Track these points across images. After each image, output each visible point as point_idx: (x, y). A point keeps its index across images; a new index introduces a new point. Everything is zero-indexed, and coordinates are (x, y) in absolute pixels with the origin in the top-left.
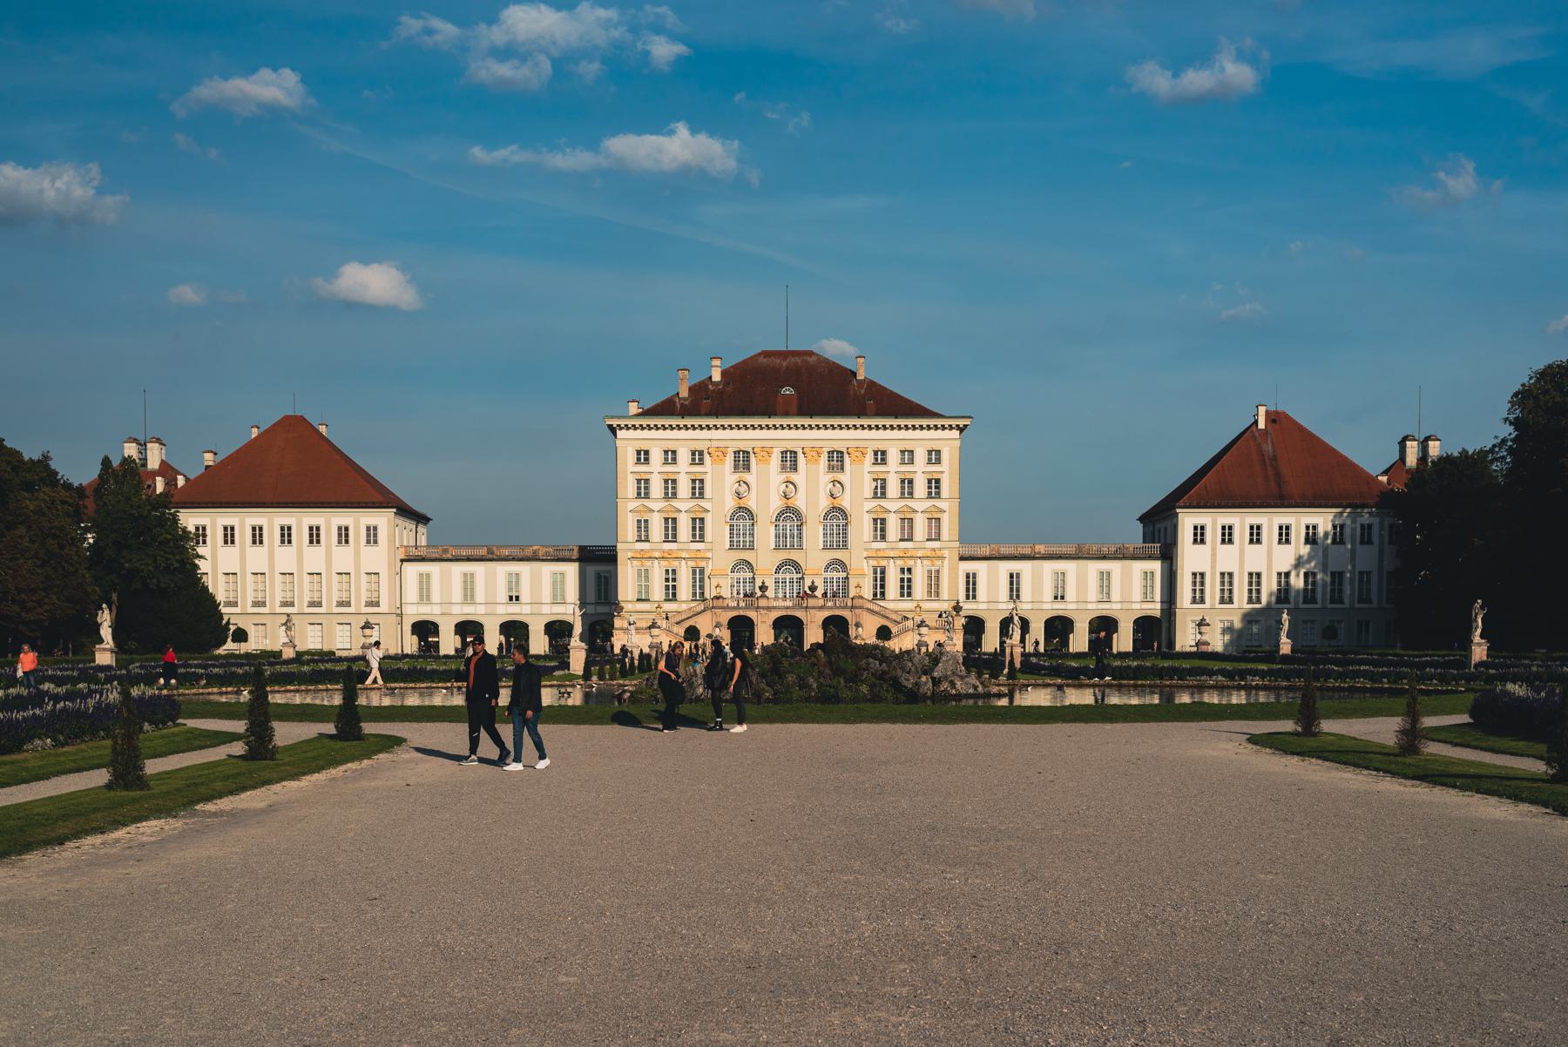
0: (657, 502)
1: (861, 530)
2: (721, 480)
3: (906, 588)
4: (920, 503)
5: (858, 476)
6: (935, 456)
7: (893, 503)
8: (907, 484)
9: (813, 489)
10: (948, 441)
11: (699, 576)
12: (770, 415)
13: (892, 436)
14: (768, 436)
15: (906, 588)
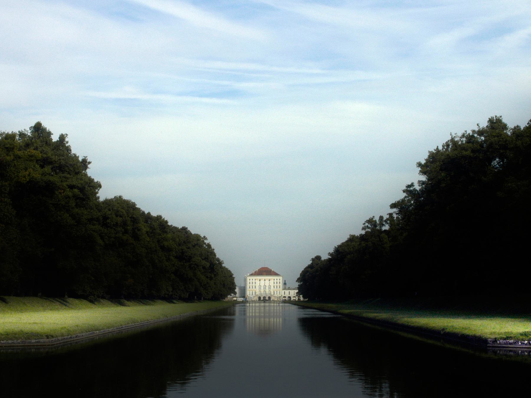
0: (251, 284)
1: (272, 287)
2: (258, 282)
3: (277, 294)
4: (278, 285)
5: (272, 282)
6: (280, 280)
7: (275, 284)
8: (277, 282)
9: (267, 283)
10: (281, 278)
11: (255, 293)
12: (263, 275)
13: (275, 278)
14: (263, 278)
15: (277, 294)
